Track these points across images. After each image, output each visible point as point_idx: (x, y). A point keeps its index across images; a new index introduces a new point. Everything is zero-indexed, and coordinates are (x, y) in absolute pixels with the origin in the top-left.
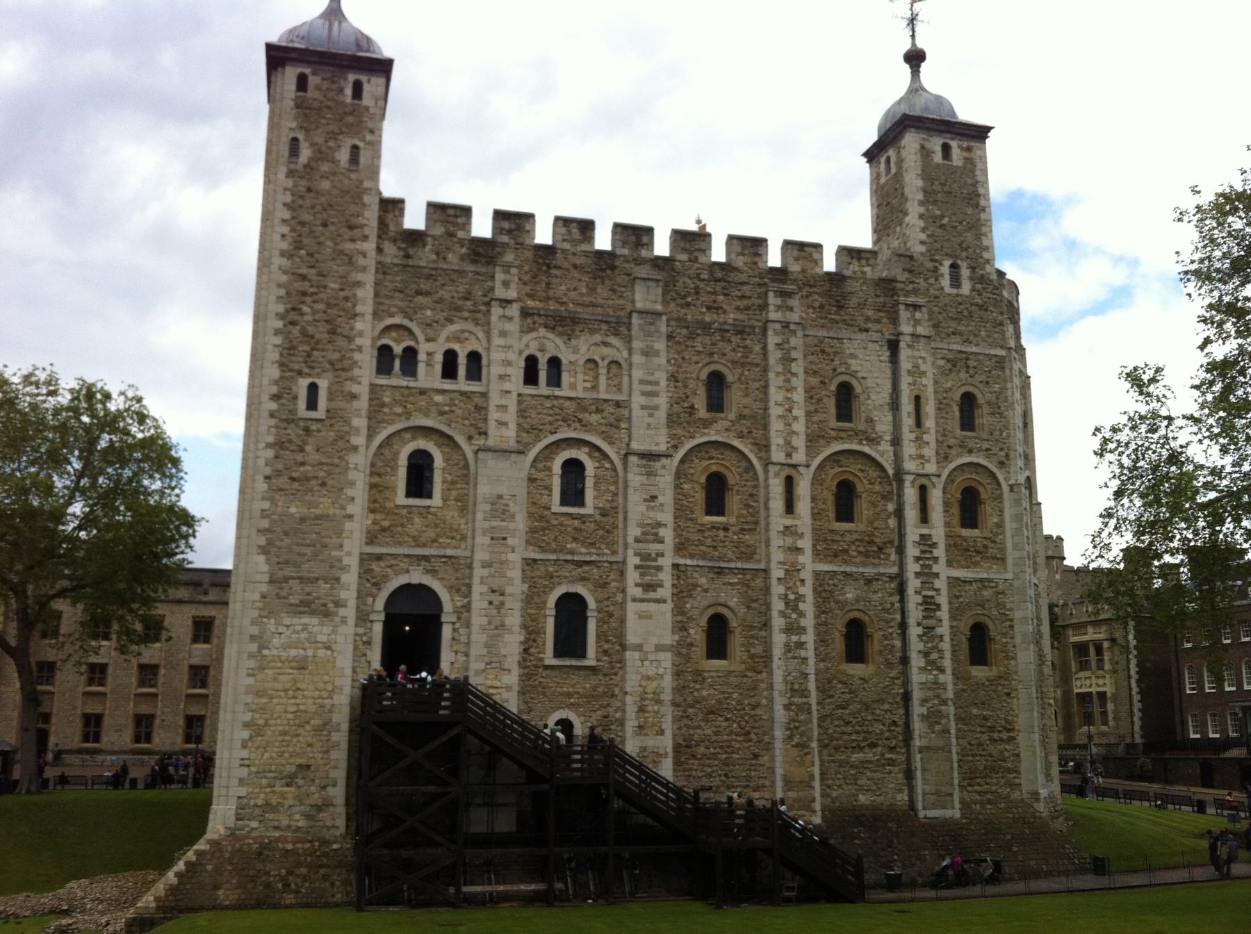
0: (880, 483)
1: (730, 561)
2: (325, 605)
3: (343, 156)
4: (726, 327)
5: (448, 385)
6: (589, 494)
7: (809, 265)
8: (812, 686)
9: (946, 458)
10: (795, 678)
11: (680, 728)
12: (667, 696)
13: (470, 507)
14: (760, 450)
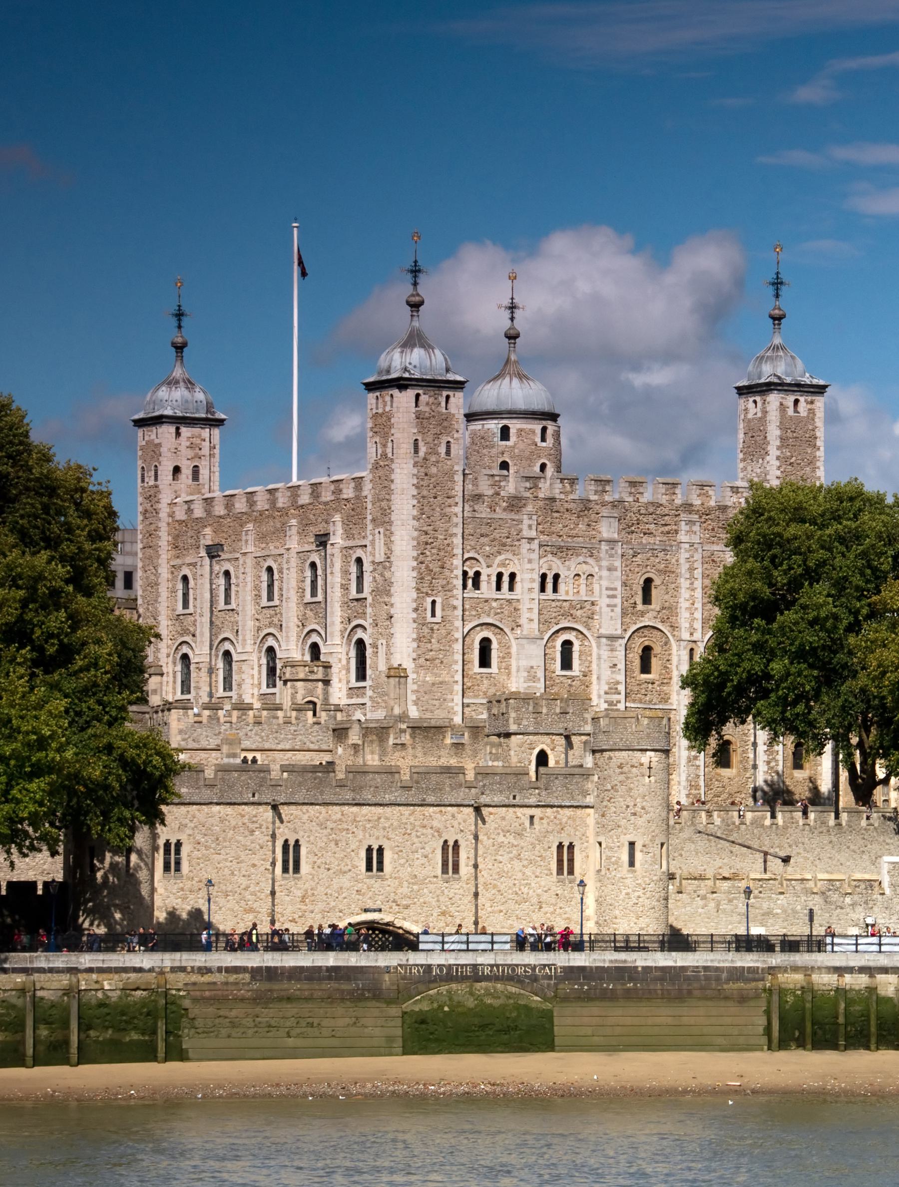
1: (655, 704)
3: (442, 450)
4: (656, 547)
7: (704, 498)
8: (702, 783)
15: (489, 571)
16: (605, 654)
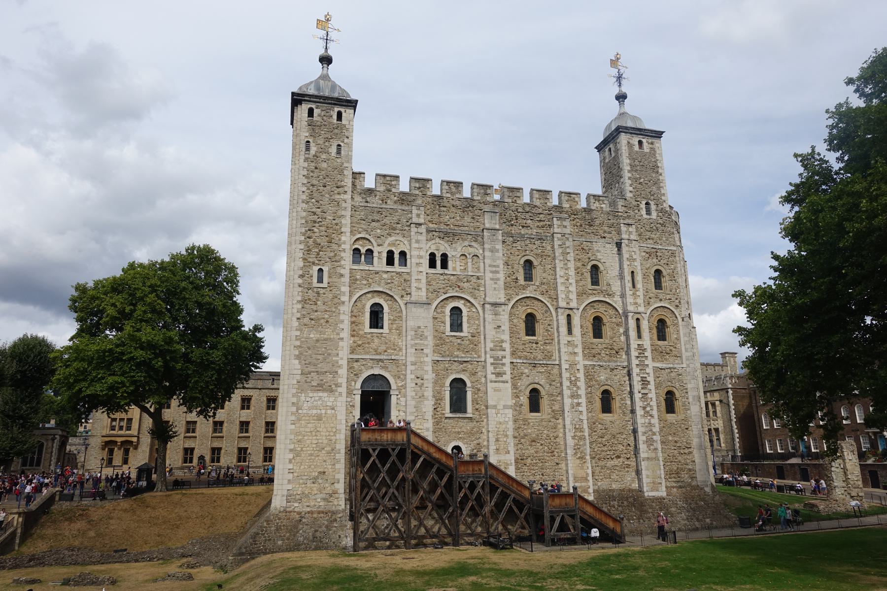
0: (615, 318)
2: (330, 386)
3: (333, 150)
4: (533, 237)
5: (390, 268)
6: (465, 325)
8: (585, 426)
9: (649, 303)
10: (577, 422)
11: (517, 450)
12: (510, 433)
13: (404, 334)
14: (553, 301)
15: (379, 249)
16: (489, 317)
